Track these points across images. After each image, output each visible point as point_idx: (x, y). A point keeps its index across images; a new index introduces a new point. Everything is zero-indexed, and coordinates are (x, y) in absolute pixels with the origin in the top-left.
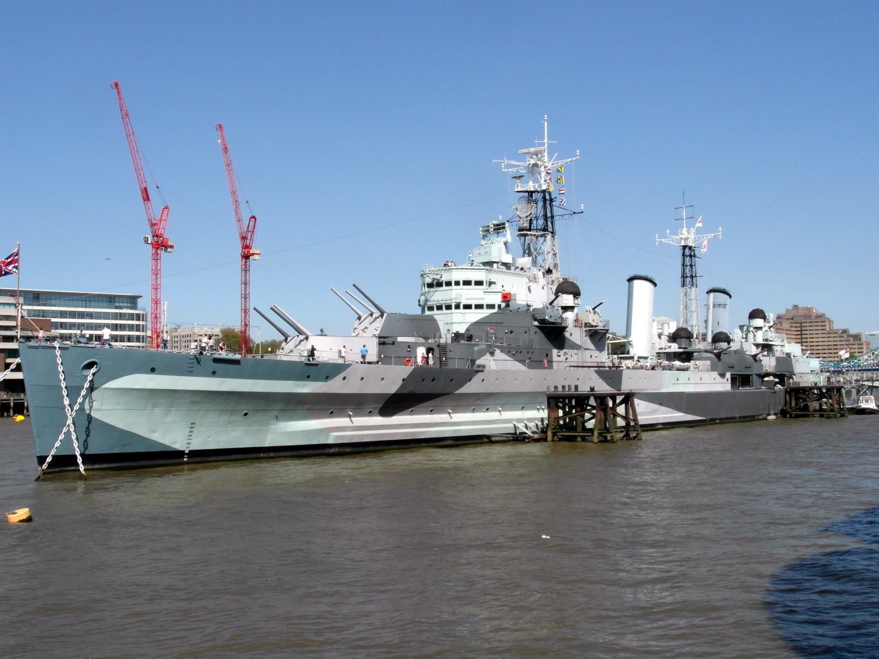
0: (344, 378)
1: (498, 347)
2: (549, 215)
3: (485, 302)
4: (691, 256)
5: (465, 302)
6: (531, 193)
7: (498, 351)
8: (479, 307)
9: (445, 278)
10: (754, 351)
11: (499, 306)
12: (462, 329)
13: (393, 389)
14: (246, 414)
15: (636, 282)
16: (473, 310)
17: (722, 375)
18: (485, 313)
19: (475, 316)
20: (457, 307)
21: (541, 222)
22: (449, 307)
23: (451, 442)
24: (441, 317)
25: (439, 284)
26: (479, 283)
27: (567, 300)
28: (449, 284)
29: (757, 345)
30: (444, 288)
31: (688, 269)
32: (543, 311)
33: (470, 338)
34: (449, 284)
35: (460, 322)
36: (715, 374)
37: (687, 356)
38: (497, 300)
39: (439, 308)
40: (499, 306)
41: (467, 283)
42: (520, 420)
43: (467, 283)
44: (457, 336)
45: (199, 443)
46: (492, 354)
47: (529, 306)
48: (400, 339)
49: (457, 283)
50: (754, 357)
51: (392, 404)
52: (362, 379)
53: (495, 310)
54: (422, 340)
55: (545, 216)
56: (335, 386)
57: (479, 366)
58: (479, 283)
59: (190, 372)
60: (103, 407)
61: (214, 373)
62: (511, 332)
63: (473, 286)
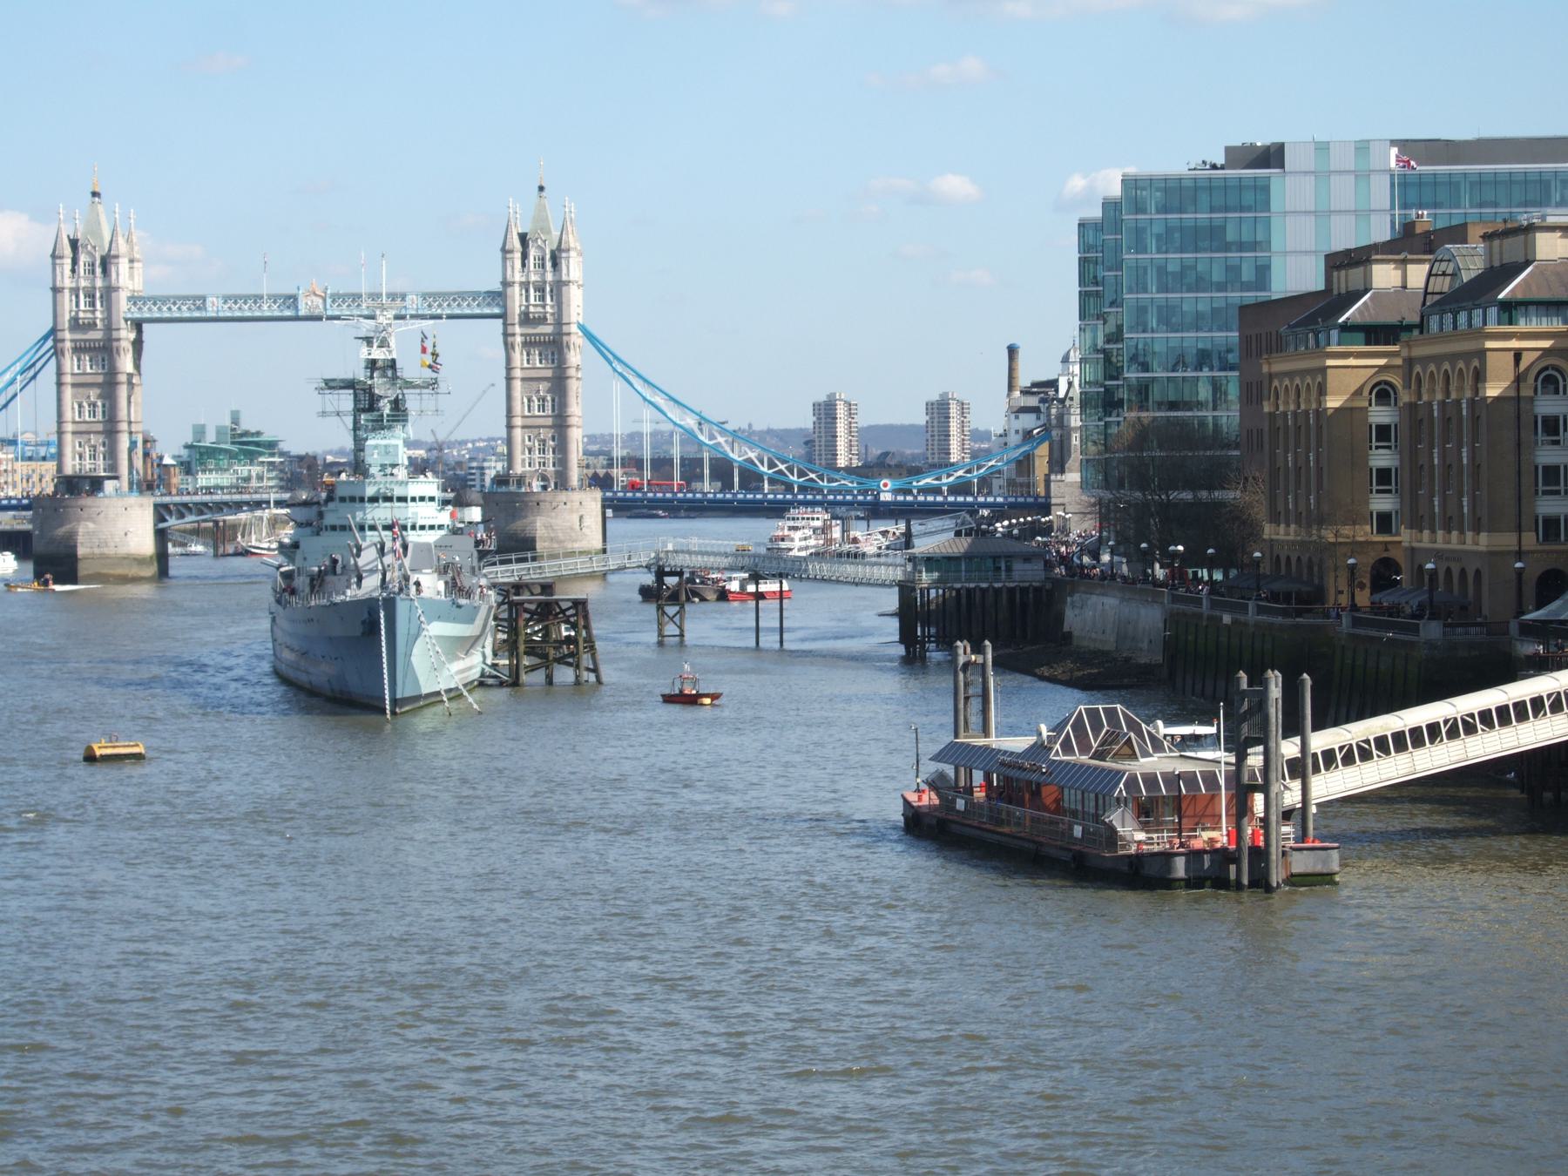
3: (436, 522)
5: (420, 522)
8: (432, 527)
9: (398, 492)
20: (413, 528)
25: (389, 499)
26: (432, 499)
28: (402, 499)
34: (402, 499)
41: (422, 499)
43: (422, 499)
49: (413, 499)
53: (443, 532)
58: (432, 499)
59: (447, 620)
61: (455, 620)
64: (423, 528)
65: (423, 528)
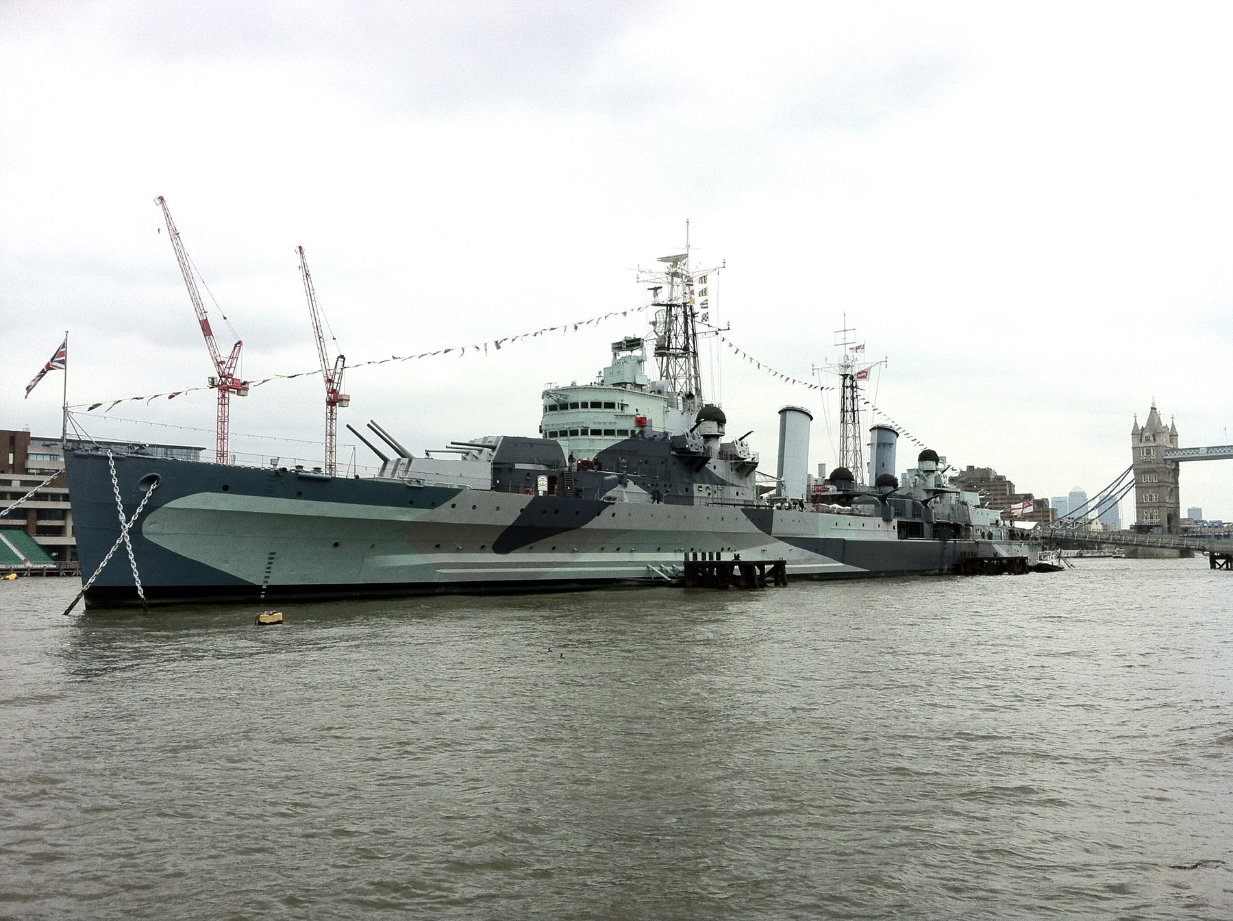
0: (453, 506)
1: (631, 478)
2: (690, 332)
3: (616, 428)
4: (852, 387)
6: (671, 306)
7: (630, 483)
8: (609, 432)
10: (924, 497)
11: (633, 432)
12: (591, 457)
13: (510, 521)
14: (336, 545)
15: (788, 414)
16: (603, 437)
17: (887, 520)
18: (619, 439)
19: (604, 443)
20: (584, 432)
21: (681, 340)
22: (574, 433)
23: (576, 586)
24: (565, 444)
25: (564, 407)
26: (610, 405)
27: (711, 427)
28: (574, 406)
29: (928, 491)
30: (570, 410)
31: (849, 401)
32: (682, 439)
33: (598, 463)
34: (574, 406)
35: (588, 449)
36: (880, 520)
37: (845, 499)
38: (630, 425)
39: (563, 434)
40: (633, 432)
41: (596, 405)
42: (656, 563)
43: (596, 405)
44: (585, 465)
45: (279, 578)
46: (625, 485)
47: (666, 434)
48: (518, 466)
49: (585, 405)
50: (925, 502)
51: (509, 539)
52: (474, 507)
54: (543, 468)
55: (686, 332)
56: (442, 514)
57: (610, 498)
58: (610, 405)
60: (165, 531)
61: (299, 495)
62: (646, 462)
63: (603, 410)
64: (596, 432)
65: (596, 432)
